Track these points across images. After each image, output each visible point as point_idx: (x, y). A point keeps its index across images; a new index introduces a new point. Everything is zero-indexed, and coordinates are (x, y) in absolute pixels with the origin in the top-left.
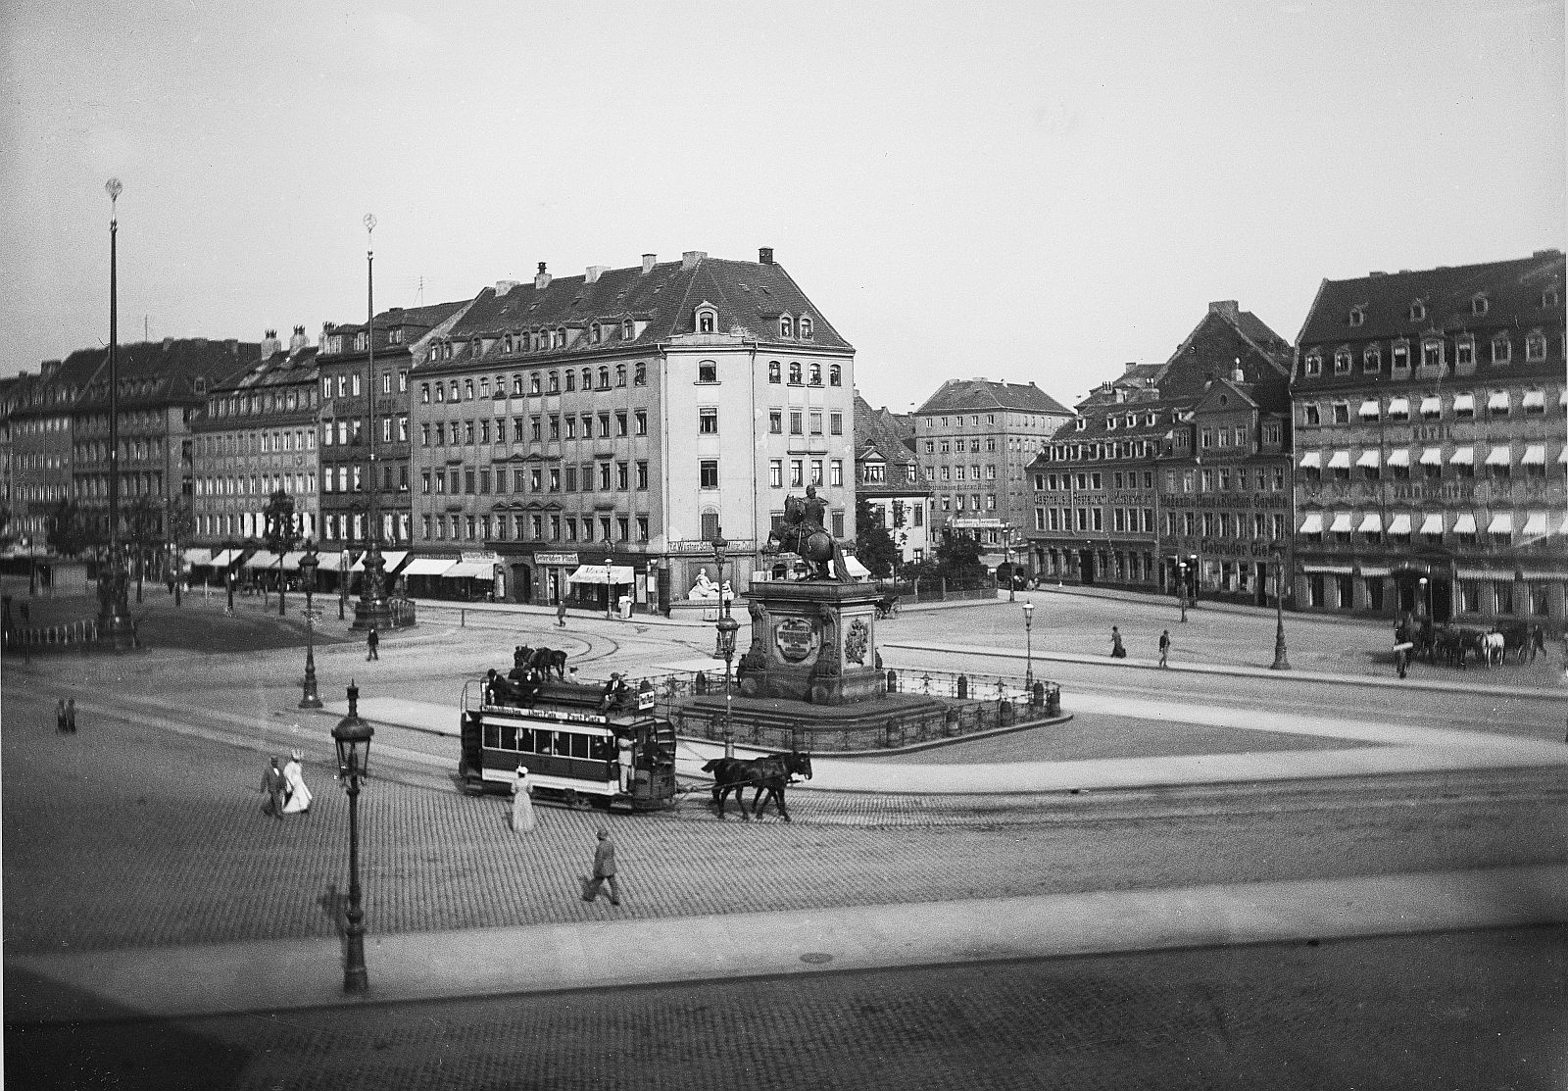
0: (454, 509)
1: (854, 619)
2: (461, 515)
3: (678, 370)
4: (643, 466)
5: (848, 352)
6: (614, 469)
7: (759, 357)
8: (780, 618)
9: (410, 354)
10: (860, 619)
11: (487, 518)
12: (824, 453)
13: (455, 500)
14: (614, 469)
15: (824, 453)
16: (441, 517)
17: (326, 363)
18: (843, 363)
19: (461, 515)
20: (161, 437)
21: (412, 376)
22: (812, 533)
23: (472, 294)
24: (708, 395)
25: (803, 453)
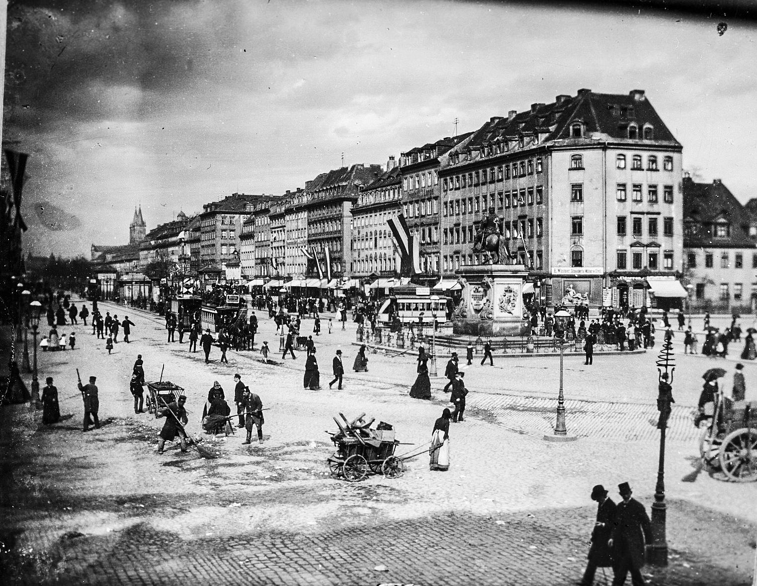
0: (457, 252)
1: (506, 286)
2: (460, 255)
3: (560, 161)
4: (540, 220)
5: (678, 149)
6: (528, 224)
7: (609, 152)
8: (473, 286)
9: (439, 162)
10: (511, 286)
11: (470, 256)
12: (659, 213)
13: (456, 247)
14: (528, 224)
15: (659, 213)
16: (451, 257)
17: (406, 170)
18: (675, 156)
19: (460, 255)
20: (339, 218)
21: (441, 174)
22: (490, 234)
23: (477, 127)
24: (577, 177)
25: (643, 213)
